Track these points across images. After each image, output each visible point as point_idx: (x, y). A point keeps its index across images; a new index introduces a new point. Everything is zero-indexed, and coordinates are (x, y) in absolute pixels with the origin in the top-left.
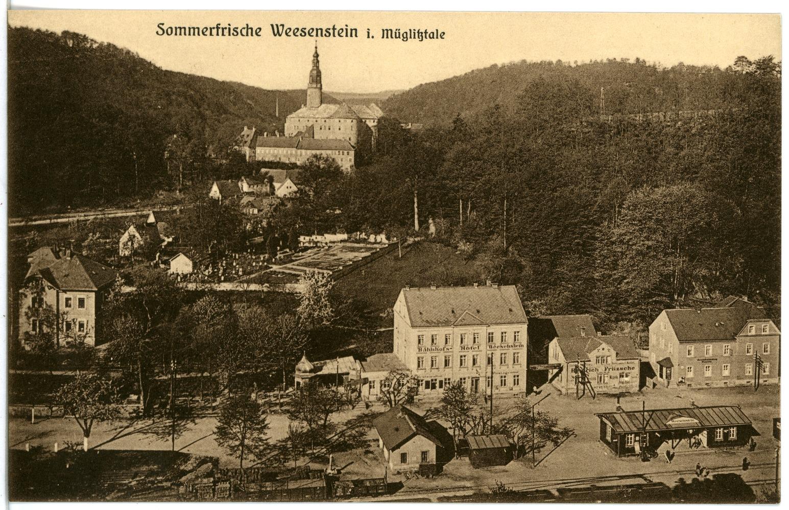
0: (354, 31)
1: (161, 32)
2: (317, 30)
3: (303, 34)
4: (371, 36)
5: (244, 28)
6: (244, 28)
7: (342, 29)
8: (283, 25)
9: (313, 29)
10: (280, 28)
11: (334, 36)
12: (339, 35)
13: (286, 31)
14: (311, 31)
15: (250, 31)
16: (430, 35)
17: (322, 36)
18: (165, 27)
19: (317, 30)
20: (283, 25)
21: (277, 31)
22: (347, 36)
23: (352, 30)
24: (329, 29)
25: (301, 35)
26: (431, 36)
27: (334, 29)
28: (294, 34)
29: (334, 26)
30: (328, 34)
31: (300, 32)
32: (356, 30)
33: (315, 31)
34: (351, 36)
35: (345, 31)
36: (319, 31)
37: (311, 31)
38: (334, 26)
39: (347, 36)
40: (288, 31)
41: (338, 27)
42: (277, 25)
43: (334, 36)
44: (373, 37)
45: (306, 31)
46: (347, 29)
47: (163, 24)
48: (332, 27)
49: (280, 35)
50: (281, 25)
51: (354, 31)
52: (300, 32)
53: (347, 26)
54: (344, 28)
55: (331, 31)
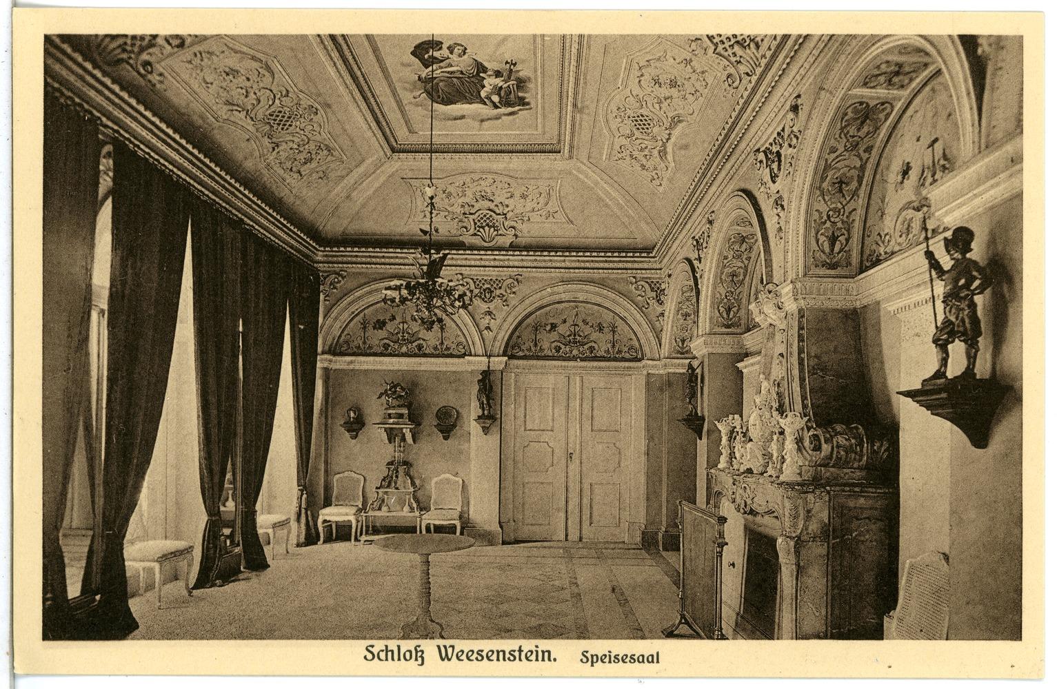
0: (546, 654)
1: (369, 656)
2: (498, 652)
3: (480, 658)
4: (552, 659)
5: (383, 651)
6: (383, 651)
7: (532, 652)
8: (453, 647)
9: (493, 652)
10: (450, 650)
11: (520, 660)
12: (527, 658)
13: (457, 655)
14: (490, 654)
15: (390, 654)
16: (405, 654)
17: (504, 660)
18: (588, 655)
19: (498, 652)
20: (453, 647)
21: (419, 656)
22: (537, 660)
23: (543, 652)
24: (514, 651)
25: (477, 659)
26: (650, 659)
27: (520, 651)
28: (468, 658)
29: (520, 647)
30: (512, 658)
31: (475, 655)
32: (549, 652)
33: (495, 653)
34: (543, 660)
35: (535, 653)
36: (501, 654)
37: (490, 654)
38: (520, 647)
39: (537, 660)
40: (460, 654)
41: (525, 649)
42: (445, 647)
43: (520, 660)
44: (555, 660)
45: (484, 654)
46: (537, 652)
47: (372, 646)
48: (517, 649)
49: (449, 660)
50: (450, 646)
51: (546, 654)
52: (475, 655)
53: (537, 647)
54: (534, 649)
55: (517, 654)
